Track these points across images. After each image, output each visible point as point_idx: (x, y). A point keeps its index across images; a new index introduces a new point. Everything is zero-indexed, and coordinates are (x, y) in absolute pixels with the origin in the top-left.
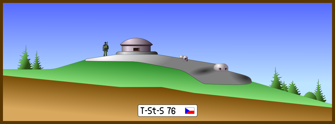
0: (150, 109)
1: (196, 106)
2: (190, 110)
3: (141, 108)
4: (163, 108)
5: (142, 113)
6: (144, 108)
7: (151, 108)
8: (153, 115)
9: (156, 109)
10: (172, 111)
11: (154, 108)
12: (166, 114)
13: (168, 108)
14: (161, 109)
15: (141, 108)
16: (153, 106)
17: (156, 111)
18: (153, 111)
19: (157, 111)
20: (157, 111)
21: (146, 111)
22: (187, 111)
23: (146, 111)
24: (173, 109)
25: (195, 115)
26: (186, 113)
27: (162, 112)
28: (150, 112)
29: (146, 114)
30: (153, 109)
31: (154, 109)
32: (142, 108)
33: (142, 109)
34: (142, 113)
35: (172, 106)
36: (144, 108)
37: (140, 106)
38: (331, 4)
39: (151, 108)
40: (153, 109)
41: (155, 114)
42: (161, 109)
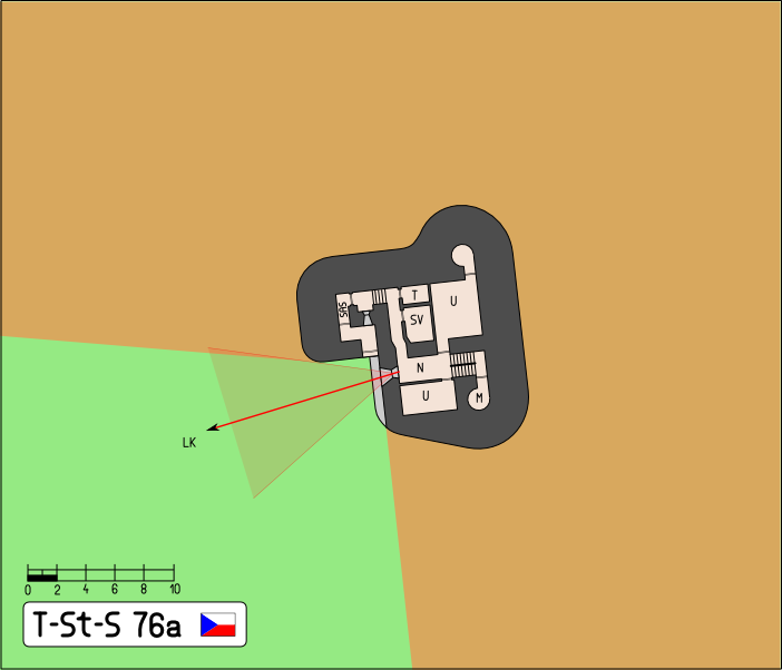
0: (67, 619)
2: (219, 620)
3: (35, 613)
4: (118, 613)
5: (40, 635)
6: (45, 613)
7: (73, 613)
9: (89, 619)
10: (152, 626)
11: (84, 613)
13: (135, 613)
14: (112, 619)
15: (35, 613)
17: (89, 625)
18: (78, 625)
19: (96, 624)
20: (96, 624)
21: (52, 624)
23: (52, 624)
24: (157, 620)
25: (239, 639)
26: (202, 634)
27: (114, 630)
28: (69, 630)
30: (78, 619)
31: (83, 618)
32: (40, 614)
33: (37, 616)
34: (40, 635)
35: (150, 609)
36: (45, 613)
37: (31, 609)
39: (73, 613)
40: (78, 619)
41: (89, 635)
42: (112, 619)
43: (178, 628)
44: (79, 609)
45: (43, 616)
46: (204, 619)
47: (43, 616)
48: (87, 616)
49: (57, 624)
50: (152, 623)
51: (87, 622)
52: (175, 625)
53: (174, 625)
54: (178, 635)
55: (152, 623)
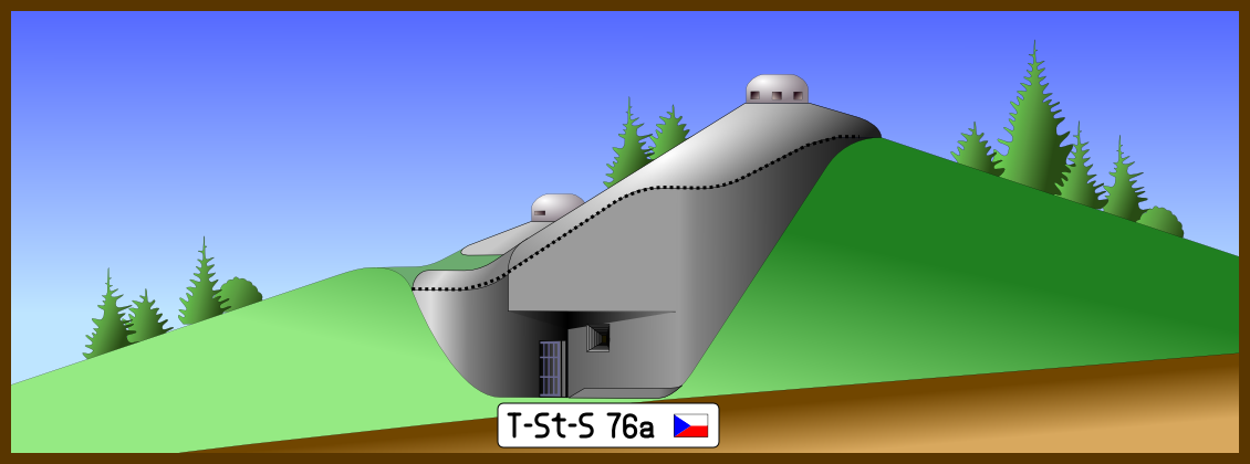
0: (541, 420)
1: (713, 409)
2: (692, 421)
3: (509, 414)
4: (592, 414)
5: (514, 436)
6: (520, 414)
7: (547, 414)
8: (553, 441)
9: (564, 420)
10: (626, 427)
11: (559, 414)
12: (602, 439)
13: (609, 414)
14: (585, 420)
15: (509, 414)
16: (553, 410)
18: (553, 426)
19: (570, 425)
20: (570, 425)
21: (526, 425)
22: (680, 428)
23: (526, 425)
24: (630, 421)
27: (587, 431)
28: (543, 431)
29: (527, 439)
30: (553, 420)
31: (558, 419)
32: (514, 415)
33: (511, 417)
34: (514, 436)
35: (624, 410)
36: (520, 414)
38: (1236, 14)
39: (547, 414)
40: (553, 420)
41: (564, 436)
42: (585, 420)
43: (651, 429)
44: (553, 410)
45: (517, 417)
46: (677, 420)
47: (517, 417)
48: (562, 417)
49: (531, 425)
50: (624, 423)
51: (562, 423)
52: (647, 426)
53: (647, 426)
54: (651, 435)
55: (624, 423)
